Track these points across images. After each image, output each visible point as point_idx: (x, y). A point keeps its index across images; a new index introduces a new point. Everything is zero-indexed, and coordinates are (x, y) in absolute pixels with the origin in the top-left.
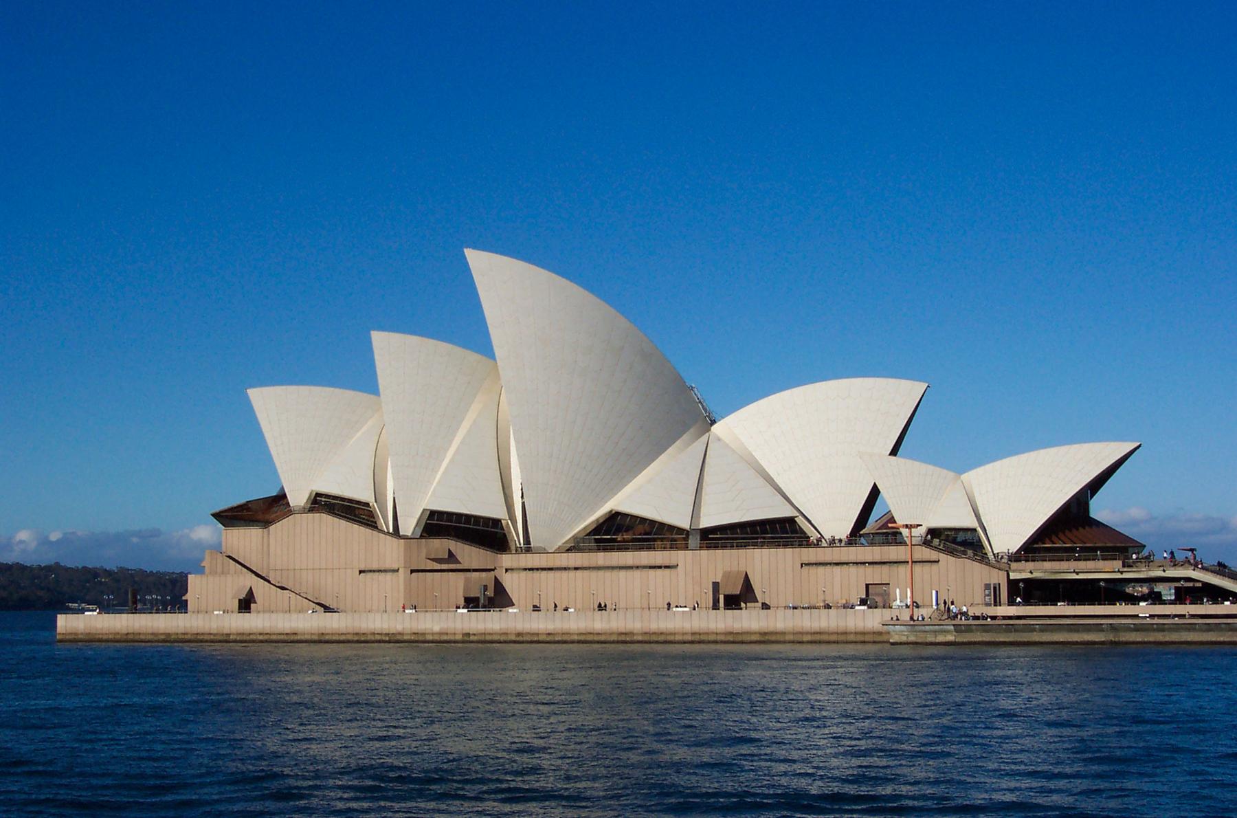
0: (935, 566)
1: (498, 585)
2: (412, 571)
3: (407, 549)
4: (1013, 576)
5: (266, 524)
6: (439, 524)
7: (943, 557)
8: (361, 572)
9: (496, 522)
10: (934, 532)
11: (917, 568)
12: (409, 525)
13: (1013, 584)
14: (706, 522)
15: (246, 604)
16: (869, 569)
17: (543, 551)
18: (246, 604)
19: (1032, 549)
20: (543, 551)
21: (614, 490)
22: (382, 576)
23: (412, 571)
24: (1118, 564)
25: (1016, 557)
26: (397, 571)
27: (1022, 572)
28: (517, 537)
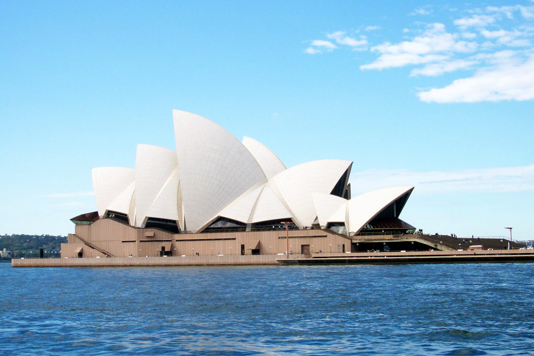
0: (325, 238)
1: (172, 247)
2: (141, 241)
3: (139, 232)
4: (354, 241)
7: (328, 234)
8: (123, 242)
9: (174, 222)
11: (291, 240)
12: (140, 223)
13: (353, 245)
14: (256, 220)
16: (303, 239)
18: (80, 255)
19: (363, 231)
20: (191, 233)
21: (221, 209)
22: (130, 243)
23: (141, 241)
24: (391, 237)
26: (135, 241)
28: (182, 227)
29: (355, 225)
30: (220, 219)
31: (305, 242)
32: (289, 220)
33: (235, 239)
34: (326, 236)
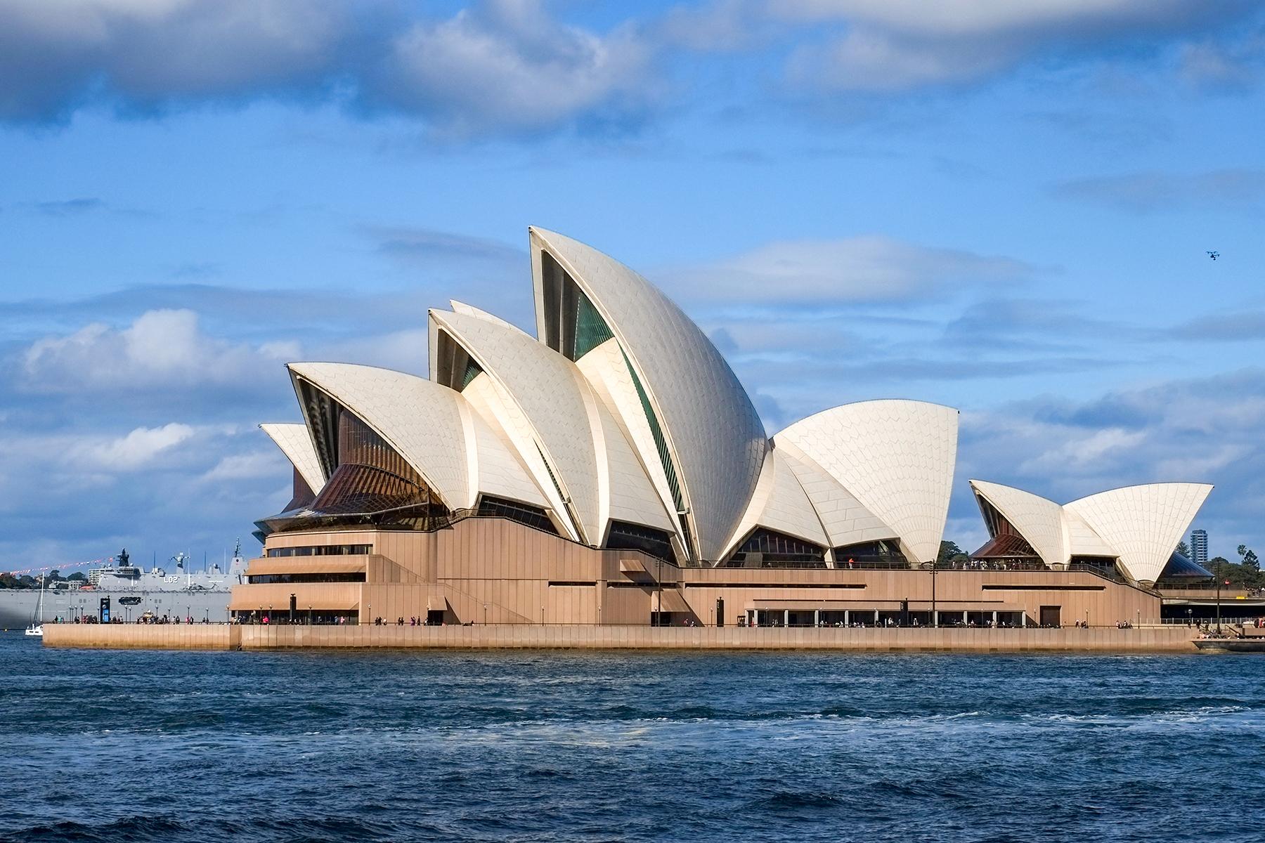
2: (609, 585)
4: (1165, 602)
5: (433, 528)
6: (623, 535)
7: (1106, 583)
8: (551, 583)
9: (663, 535)
10: (1078, 562)
14: (838, 542)
15: (436, 618)
17: (707, 565)
18: (436, 618)
25: (1156, 586)
26: (593, 584)
27: (1175, 597)
29: (1144, 563)
30: (760, 535)
31: (1050, 598)
32: (893, 544)
33: (863, 586)
34: (1102, 588)
